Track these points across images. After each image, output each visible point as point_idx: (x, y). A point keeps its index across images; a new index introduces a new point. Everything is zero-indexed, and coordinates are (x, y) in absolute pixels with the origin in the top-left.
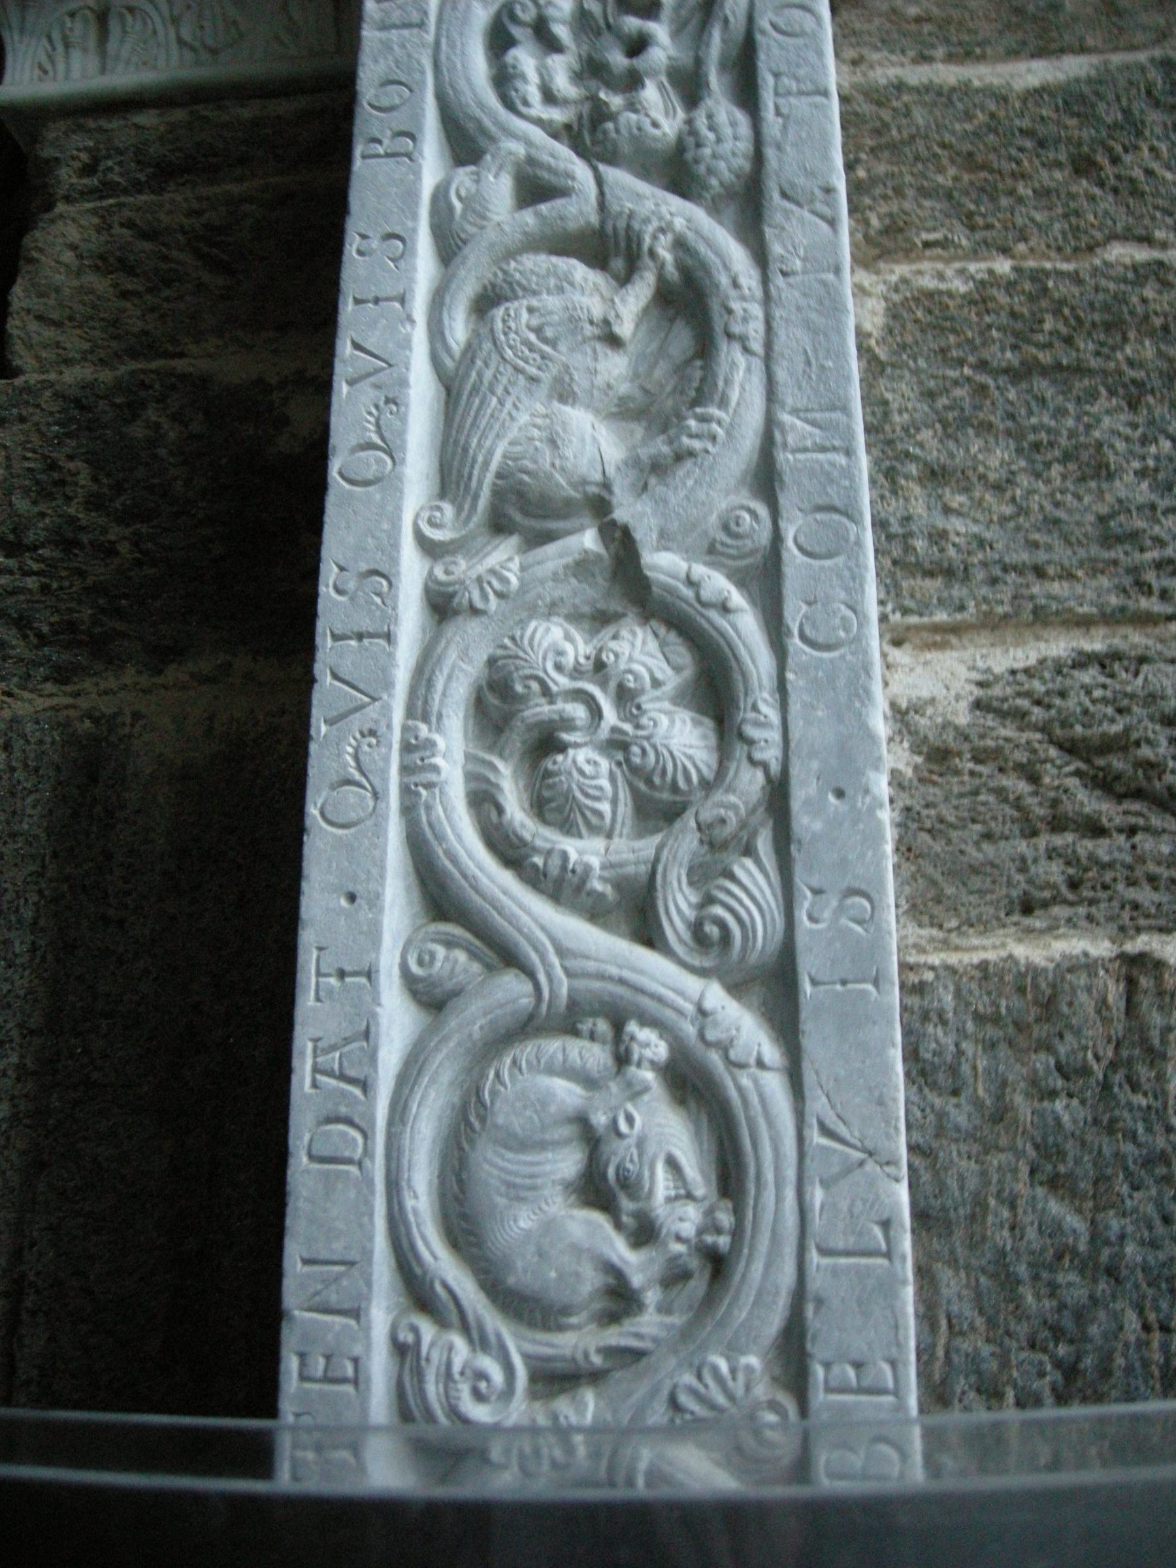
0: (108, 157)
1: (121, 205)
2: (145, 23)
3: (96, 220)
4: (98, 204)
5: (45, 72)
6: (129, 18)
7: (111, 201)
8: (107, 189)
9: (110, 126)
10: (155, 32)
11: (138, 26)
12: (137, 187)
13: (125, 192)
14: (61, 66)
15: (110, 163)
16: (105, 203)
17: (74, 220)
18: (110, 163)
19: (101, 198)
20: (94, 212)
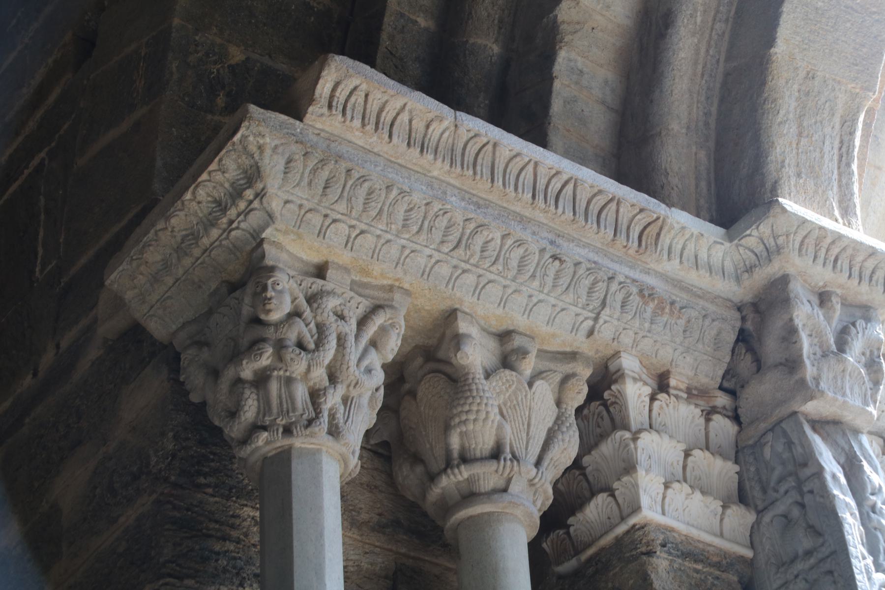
8: (670, 554)
12: (678, 557)
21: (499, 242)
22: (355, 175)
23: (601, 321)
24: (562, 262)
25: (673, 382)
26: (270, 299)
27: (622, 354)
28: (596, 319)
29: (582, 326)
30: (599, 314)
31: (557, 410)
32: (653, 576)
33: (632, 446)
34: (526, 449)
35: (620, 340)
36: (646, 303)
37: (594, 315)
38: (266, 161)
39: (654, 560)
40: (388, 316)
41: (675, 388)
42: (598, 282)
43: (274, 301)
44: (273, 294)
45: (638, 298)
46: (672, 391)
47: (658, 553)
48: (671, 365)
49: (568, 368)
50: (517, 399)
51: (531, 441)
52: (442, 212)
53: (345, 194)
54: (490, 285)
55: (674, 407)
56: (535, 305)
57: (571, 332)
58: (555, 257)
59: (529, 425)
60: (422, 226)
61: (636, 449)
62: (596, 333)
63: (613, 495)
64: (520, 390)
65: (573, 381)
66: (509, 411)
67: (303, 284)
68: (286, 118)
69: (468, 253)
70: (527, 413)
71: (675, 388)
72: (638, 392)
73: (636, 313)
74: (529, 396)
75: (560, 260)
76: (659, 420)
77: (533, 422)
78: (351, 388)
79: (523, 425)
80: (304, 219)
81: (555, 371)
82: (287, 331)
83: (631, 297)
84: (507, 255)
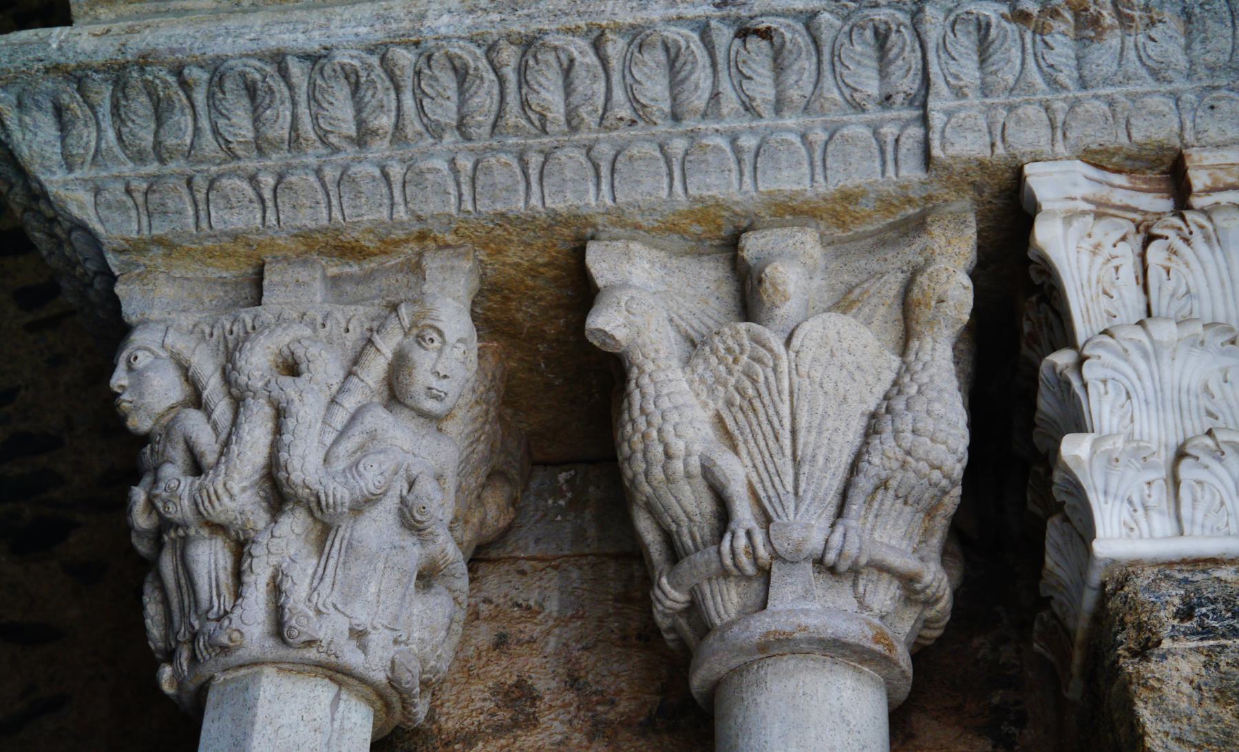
0: (1202, 605)
1: (1225, 647)
2: (1213, 495)
3: (1203, 658)
4: (1200, 644)
5: (1132, 529)
6: (1198, 488)
7: (1212, 642)
8: (1205, 632)
9: (1195, 579)
10: (1222, 503)
11: (1208, 496)
13: (1224, 636)
14: (1144, 526)
15: (1204, 610)
16: (1207, 643)
17: (1183, 657)
18: (1204, 610)
19: (1202, 639)
20: (1197, 650)
21: (591, 59)
22: (196, 74)
23: (937, 119)
24: (766, 34)
25: (1199, 179)
26: (118, 395)
27: (1028, 169)
28: (925, 120)
29: (903, 150)
30: (924, 106)
31: (896, 362)
32: (1145, 713)
33: (1076, 384)
34: (796, 494)
35: (1009, 139)
36: (1040, 30)
37: (917, 113)
38: (17, 135)
39: (1153, 667)
40: (406, 323)
41: (1209, 191)
42: (886, 37)
43: (126, 397)
44: (125, 382)
45: (1011, 28)
46: (1197, 202)
47: (1166, 644)
48: (1181, 137)
49: (911, 253)
50: (754, 382)
51: (805, 469)
52: (423, 59)
53: (204, 123)
54: (620, 158)
55: (1207, 239)
56: (757, 155)
57: (883, 173)
58: (743, 33)
59: (794, 432)
60: (399, 109)
61: (1085, 386)
62: (936, 151)
63: (1066, 519)
64: (759, 360)
65: (923, 279)
66: (740, 416)
67: (215, 333)
68: (32, 32)
69: (534, 117)
70: (785, 410)
71: (1209, 191)
72: (1087, 244)
73: (1023, 63)
74: (784, 366)
75: (757, 32)
76: (1169, 286)
77: (803, 422)
78: (318, 515)
79: (777, 439)
80: (151, 208)
81: (883, 275)
82: (165, 446)
83: (993, 32)
84: (629, 80)
